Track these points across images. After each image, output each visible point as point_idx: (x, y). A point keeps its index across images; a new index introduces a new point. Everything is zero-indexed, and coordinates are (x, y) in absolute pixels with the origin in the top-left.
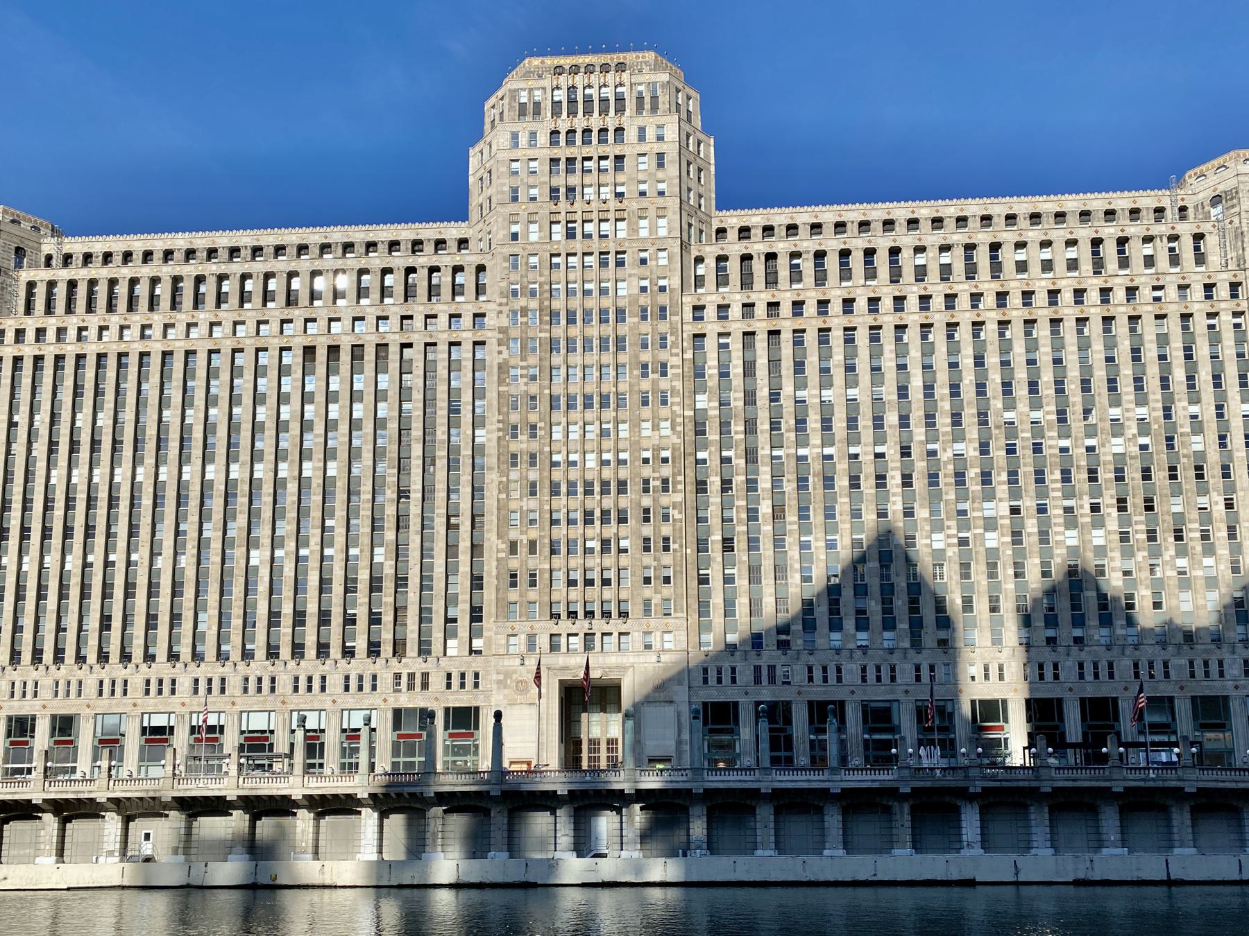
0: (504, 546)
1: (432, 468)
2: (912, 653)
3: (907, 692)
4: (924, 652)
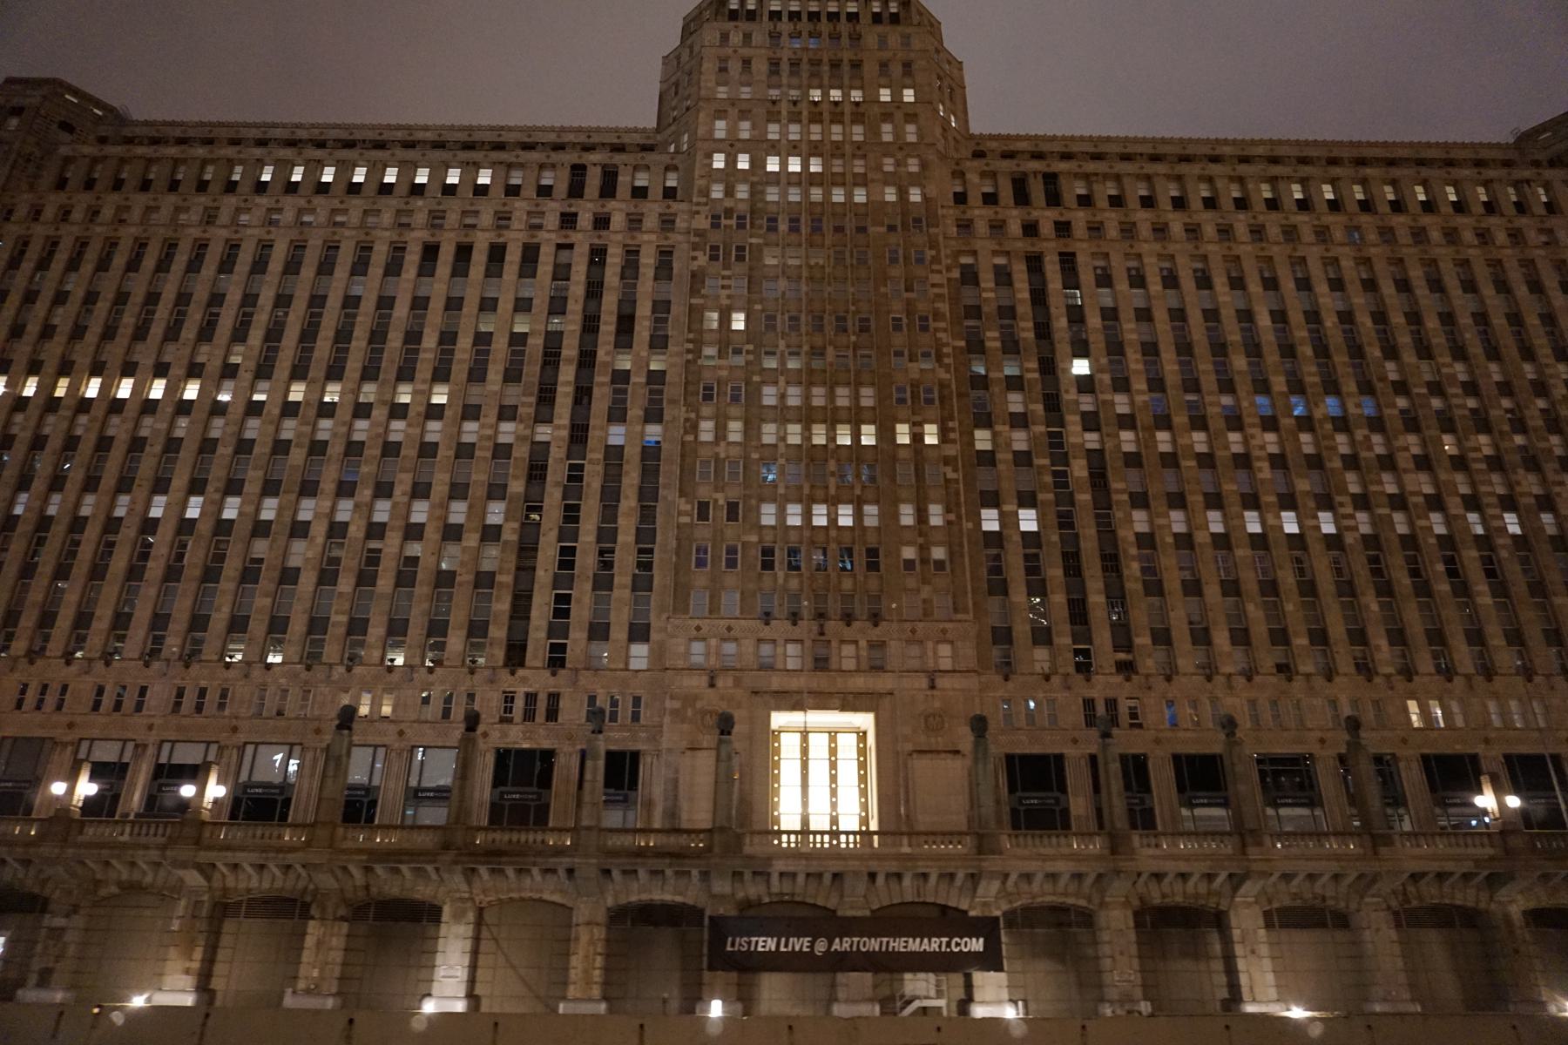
0: (688, 507)
1: (585, 400)
2: (1319, 681)
3: (1322, 741)
4: (1337, 679)
